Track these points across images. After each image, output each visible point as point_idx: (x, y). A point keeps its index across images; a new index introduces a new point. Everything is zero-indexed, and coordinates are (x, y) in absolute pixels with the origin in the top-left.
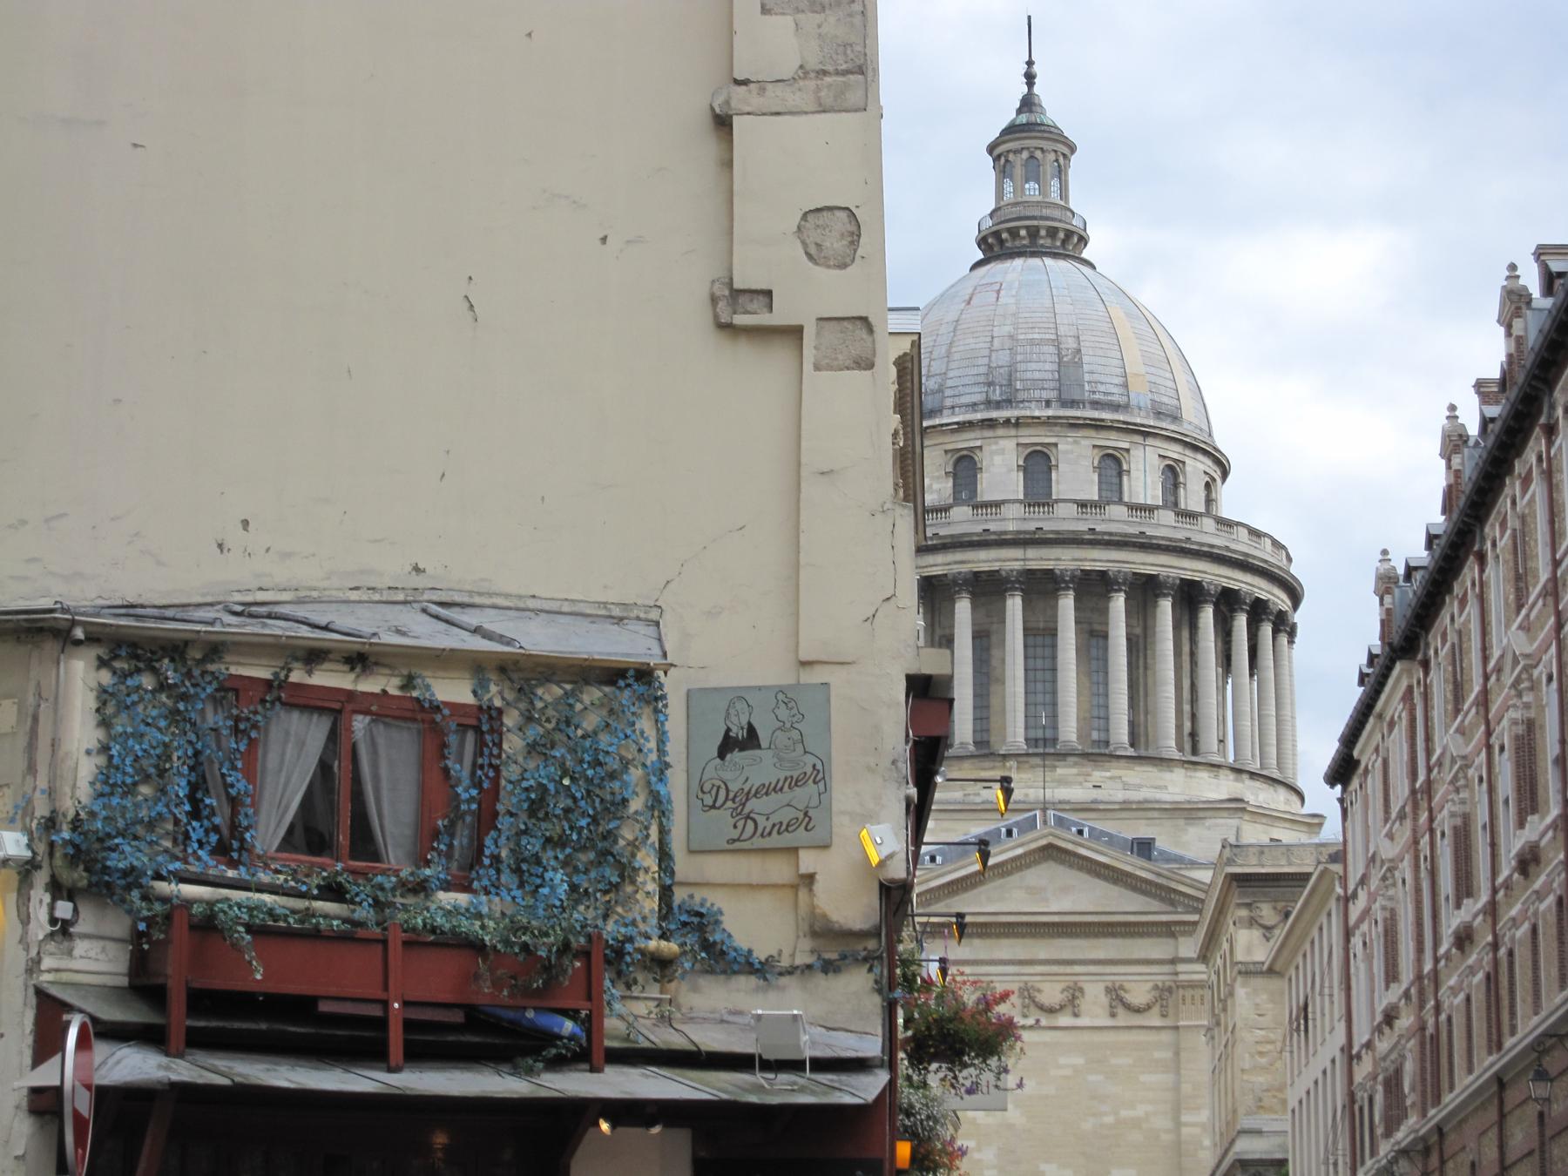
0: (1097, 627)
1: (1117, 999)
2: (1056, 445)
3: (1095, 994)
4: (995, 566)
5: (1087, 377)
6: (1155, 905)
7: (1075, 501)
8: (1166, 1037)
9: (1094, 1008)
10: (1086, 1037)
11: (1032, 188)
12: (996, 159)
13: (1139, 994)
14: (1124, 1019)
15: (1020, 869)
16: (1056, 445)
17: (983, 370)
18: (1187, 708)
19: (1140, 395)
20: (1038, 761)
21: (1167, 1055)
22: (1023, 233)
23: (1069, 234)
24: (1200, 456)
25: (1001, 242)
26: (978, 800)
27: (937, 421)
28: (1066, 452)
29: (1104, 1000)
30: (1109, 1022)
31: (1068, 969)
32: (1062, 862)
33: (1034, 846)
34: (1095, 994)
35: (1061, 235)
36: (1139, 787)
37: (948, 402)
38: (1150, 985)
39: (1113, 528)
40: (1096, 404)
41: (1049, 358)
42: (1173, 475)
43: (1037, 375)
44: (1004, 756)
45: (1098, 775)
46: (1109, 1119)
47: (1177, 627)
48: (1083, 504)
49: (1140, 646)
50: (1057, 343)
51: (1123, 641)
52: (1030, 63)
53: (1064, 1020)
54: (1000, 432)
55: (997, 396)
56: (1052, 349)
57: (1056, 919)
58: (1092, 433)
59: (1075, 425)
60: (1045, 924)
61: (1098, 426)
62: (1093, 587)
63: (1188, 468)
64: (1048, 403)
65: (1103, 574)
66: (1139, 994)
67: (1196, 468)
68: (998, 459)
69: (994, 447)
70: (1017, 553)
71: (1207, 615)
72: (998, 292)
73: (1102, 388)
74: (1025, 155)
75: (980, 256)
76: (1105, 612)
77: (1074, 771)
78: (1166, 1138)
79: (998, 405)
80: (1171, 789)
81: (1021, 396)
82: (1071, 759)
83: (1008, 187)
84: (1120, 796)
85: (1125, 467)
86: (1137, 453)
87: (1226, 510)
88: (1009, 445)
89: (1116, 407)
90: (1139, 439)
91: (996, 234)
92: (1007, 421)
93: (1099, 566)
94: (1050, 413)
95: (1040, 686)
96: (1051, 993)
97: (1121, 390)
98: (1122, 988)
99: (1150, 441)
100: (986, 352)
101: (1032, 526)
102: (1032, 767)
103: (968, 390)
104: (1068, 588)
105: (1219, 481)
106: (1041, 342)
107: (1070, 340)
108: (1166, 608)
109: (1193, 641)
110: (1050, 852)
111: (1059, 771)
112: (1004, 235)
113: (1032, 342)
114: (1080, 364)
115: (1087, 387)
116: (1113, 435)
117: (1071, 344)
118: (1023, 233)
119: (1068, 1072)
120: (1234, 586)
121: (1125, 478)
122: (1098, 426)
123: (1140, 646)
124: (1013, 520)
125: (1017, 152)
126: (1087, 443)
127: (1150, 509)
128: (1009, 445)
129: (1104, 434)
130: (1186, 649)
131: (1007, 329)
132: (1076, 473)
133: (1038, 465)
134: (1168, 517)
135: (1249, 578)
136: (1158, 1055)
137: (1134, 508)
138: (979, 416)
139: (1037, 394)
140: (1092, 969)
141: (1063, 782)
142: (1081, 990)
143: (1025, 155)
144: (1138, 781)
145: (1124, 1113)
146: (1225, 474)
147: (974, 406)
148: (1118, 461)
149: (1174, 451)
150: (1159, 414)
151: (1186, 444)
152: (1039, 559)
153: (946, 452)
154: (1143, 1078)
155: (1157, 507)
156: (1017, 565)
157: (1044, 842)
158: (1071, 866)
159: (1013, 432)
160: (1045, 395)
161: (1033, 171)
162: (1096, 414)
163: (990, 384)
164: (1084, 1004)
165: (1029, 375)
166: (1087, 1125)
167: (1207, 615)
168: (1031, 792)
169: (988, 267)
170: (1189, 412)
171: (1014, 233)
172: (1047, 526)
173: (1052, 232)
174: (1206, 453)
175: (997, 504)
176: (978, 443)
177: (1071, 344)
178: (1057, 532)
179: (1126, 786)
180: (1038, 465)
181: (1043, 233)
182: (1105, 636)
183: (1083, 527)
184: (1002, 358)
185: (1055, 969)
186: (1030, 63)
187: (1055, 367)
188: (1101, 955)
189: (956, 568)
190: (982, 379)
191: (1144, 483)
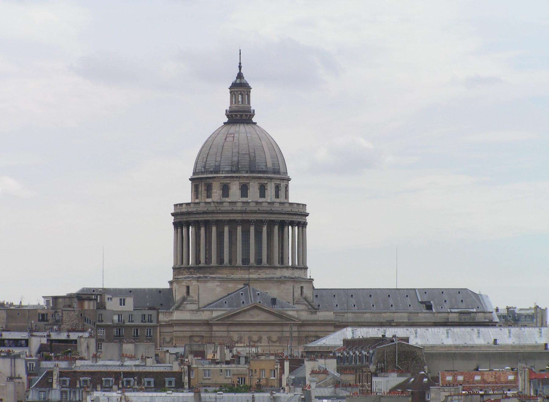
1: (269, 339)
3: (265, 338)
5: (257, 164)
6: (278, 319)
12: (231, 92)
13: (274, 338)
14: (271, 344)
17: (230, 161)
18: (280, 251)
19: (270, 165)
23: (250, 115)
27: (218, 175)
29: (267, 340)
30: (268, 345)
34: (265, 338)
40: (260, 172)
42: (277, 188)
50: (249, 154)
52: (240, 63)
54: (235, 179)
55: (234, 169)
64: (247, 173)
67: (283, 184)
68: (234, 187)
72: (233, 137)
75: (226, 120)
79: (234, 172)
81: (240, 169)
84: (265, 276)
86: (269, 184)
87: (291, 201)
88: (237, 183)
89: (264, 172)
90: (269, 180)
91: (232, 115)
92: (237, 177)
96: (255, 338)
99: (273, 180)
101: (244, 208)
106: (246, 154)
110: (256, 307)
113: (243, 154)
116: (263, 180)
117: (253, 155)
120: (293, 220)
124: (239, 207)
126: (257, 182)
128: (237, 183)
131: (236, 150)
135: (297, 217)
138: (229, 175)
149: (278, 182)
150: (274, 173)
152: (246, 217)
156: (240, 218)
160: (247, 169)
170: (282, 170)
172: (248, 209)
175: (236, 202)
177: (253, 155)
183: (256, 209)
184: (235, 159)
186: (240, 63)
188: (266, 330)
190: (230, 164)
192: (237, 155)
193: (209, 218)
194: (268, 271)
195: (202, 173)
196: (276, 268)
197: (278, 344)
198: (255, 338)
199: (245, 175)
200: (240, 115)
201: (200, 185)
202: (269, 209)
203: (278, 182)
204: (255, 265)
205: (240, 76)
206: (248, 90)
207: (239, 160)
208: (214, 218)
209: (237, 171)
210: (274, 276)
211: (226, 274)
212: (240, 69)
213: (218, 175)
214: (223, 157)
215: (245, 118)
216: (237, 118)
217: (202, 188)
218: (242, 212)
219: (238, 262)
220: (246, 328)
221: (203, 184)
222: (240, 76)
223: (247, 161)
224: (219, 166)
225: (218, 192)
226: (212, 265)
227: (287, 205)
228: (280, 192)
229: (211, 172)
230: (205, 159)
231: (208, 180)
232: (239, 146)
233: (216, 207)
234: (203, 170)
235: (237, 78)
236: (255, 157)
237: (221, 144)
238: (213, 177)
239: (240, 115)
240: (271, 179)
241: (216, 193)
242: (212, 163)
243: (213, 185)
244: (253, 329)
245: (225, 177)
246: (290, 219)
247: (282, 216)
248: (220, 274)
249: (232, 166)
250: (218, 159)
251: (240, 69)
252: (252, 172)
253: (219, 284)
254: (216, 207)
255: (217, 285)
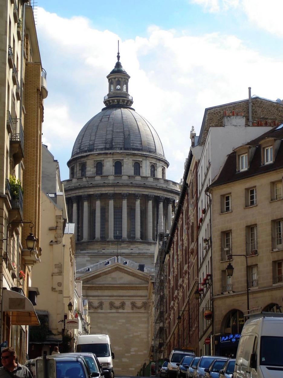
0: (133, 207)
1: (133, 305)
2: (123, 160)
3: (128, 303)
4: (107, 192)
5: (131, 142)
7: (127, 176)
8: (146, 315)
9: (128, 308)
10: (126, 315)
11: (118, 87)
12: (109, 80)
13: (139, 303)
14: (135, 310)
15: (110, 273)
16: (123, 160)
17: (104, 139)
18: (155, 228)
20: (116, 243)
21: (146, 319)
22: (116, 101)
23: (128, 101)
24: (161, 162)
25: (110, 103)
26: (101, 252)
27: (92, 153)
28: (126, 162)
29: (130, 306)
31: (122, 298)
32: (120, 271)
33: (113, 267)
34: (128, 303)
35: (126, 102)
36: (142, 249)
37: (95, 148)
38: (141, 302)
39: (137, 182)
40: (134, 149)
41: (122, 137)
42: (153, 168)
43: (118, 141)
44: (108, 241)
45: (132, 246)
46: (131, 335)
47: (153, 208)
48: (129, 177)
49: (144, 213)
50: (124, 132)
51: (139, 212)
52: (118, 53)
53: (121, 311)
54: (109, 156)
55: (108, 146)
56: (122, 134)
57: (119, 285)
58: (133, 157)
59: (128, 155)
60: (116, 287)
61: (134, 155)
62: (132, 198)
63: (157, 165)
64: (121, 149)
65: (134, 194)
66: (139, 303)
67: (160, 165)
68: (108, 163)
69: (107, 160)
70: (112, 189)
71: (161, 205)
72: (109, 118)
73: (135, 145)
74: (117, 79)
75: (104, 106)
76: (135, 204)
77: (126, 245)
78: (145, 340)
79: (108, 149)
80: (151, 250)
81: (114, 146)
82: (125, 242)
83: (112, 87)
84: (138, 252)
85: (141, 165)
86: (144, 162)
87: (167, 178)
89: (138, 150)
90: (145, 158)
91: (109, 101)
92: (110, 153)
93: (133, 192)
94: (122, 151)
95: (118, 223)
96: (117, 303)
97: (141, 145)
98: (135, 303)
99: (148, 159)
100: (105, 135)
102: (115, 244)
103: (100, 145)
104: (125, 198)
105: (166, 168)
106: (120, 132)
107: (127, 132)
108: (150, 204)
109: (158, 211)
111: (122, 245)
112: (111, 101)
113: (117, 132)
114: (129, 138)
115: (131, 144)
116: (138, 157)
117: (127, 133)
118: (116, 101)
119: (121, 324)
120: (168, 197)
121: (141, 168)
122: (134, 155)
123: (144, 213)
125: (115, 78)
126: (131, 159)
127: (147, 178)
129: (136, 157)
130: (156, 213)
131: (111, 129)
132: (128, 167)
133: (118, 166)
134: (151, 179)
136: (143, 319)
137: (142, 177)
138: (103, 152)
139: (118, 146)
140: (127, 298)
141: (123, 248)
142: (125, 303)
143: (117, 79)
144: (142, 248)
145: (135, 334)
146: (168, 165)
147: (102, 149)
148: (139, 164)
149: (154, 161)
151: (157, 159)
152: (118, 190)
153: (94, 161)
154: (140, 325)
155: (149, 177)
156: (112, 192)
157: (116, 266)
158: (123, 272)
159: (112, 156)
160: (120, 146)
161: (119, 83)
162: (134, 152)
163: (106, 143)
164: (126, 307)
165: (116, 141)
166: (126, 337)
167: (161, 205)
168: (115, 250)
169: (106, 110)
171: (113, 101)
173: (123, 101)
174: (162, 161)
175: (107, 176)
176: (103, 159)
177: (127, 133)
178: (122, 184)
179: (139, 249)
180: (118, 166)
181: (121, 101)
182: (135, 210)
183: (129, 182)
184: (109, 137)
185: (118, 298)
186: (118, 53)
187: (123, 139)
189: (97, 192)
190: (104, 142)
191: (146, 170)
192: (111, 133)
193: (81, 194)
194: (141, 246)
195: (77, 153)
196: (149, 244)
197: (142, 310)
198: (117, 303)
199: (118, 151)
200: (118, 100)
201: (75, 166)
202: (142, 183)
203: (154, 161)
204: (127, 240)
205: (118, 65)
206: (127, 78)
207: (113, 138)
208: (86, 193)
209: (111, 148)
210: (147, 251)
211: (97, 249)
212: (119, 59)
213: (92, 153)
214: (97, 135)
215: (122, 103)
216: (114, 103)
217: (77, 169)
218: (113, 185)
219: (110, 237)
220: (107, 293)
221: (78, 165)
222: (118, 65)
223: (122, 139)
224: (93, 144)
225: (92, 170)
226: (83, 240)
227: (162, 181)
228: (156, 171)
229: (86, 151)
230: (80, 141)
231: (83, 159)
232: (114, 124)
233: (87, 181)
234: (78, 151)
235: (115, 67)
236: (129, 135)
237: (97, 124)
238: (87, 156)
239: (118, 100)
240: (146, 157)
241: (90, 171)
242: (86, 142)
243: (87, 164)
244: (115, 293)
245: (99, 154)
246: (166, 196)
247: (156, 191)
248: (90, 249)
249: (106, 143)
250: (93, 138)
251: (119, 59)
252: (127, 149)
253: (89, 259)
254: (87, 181)
255: (87, 261)
